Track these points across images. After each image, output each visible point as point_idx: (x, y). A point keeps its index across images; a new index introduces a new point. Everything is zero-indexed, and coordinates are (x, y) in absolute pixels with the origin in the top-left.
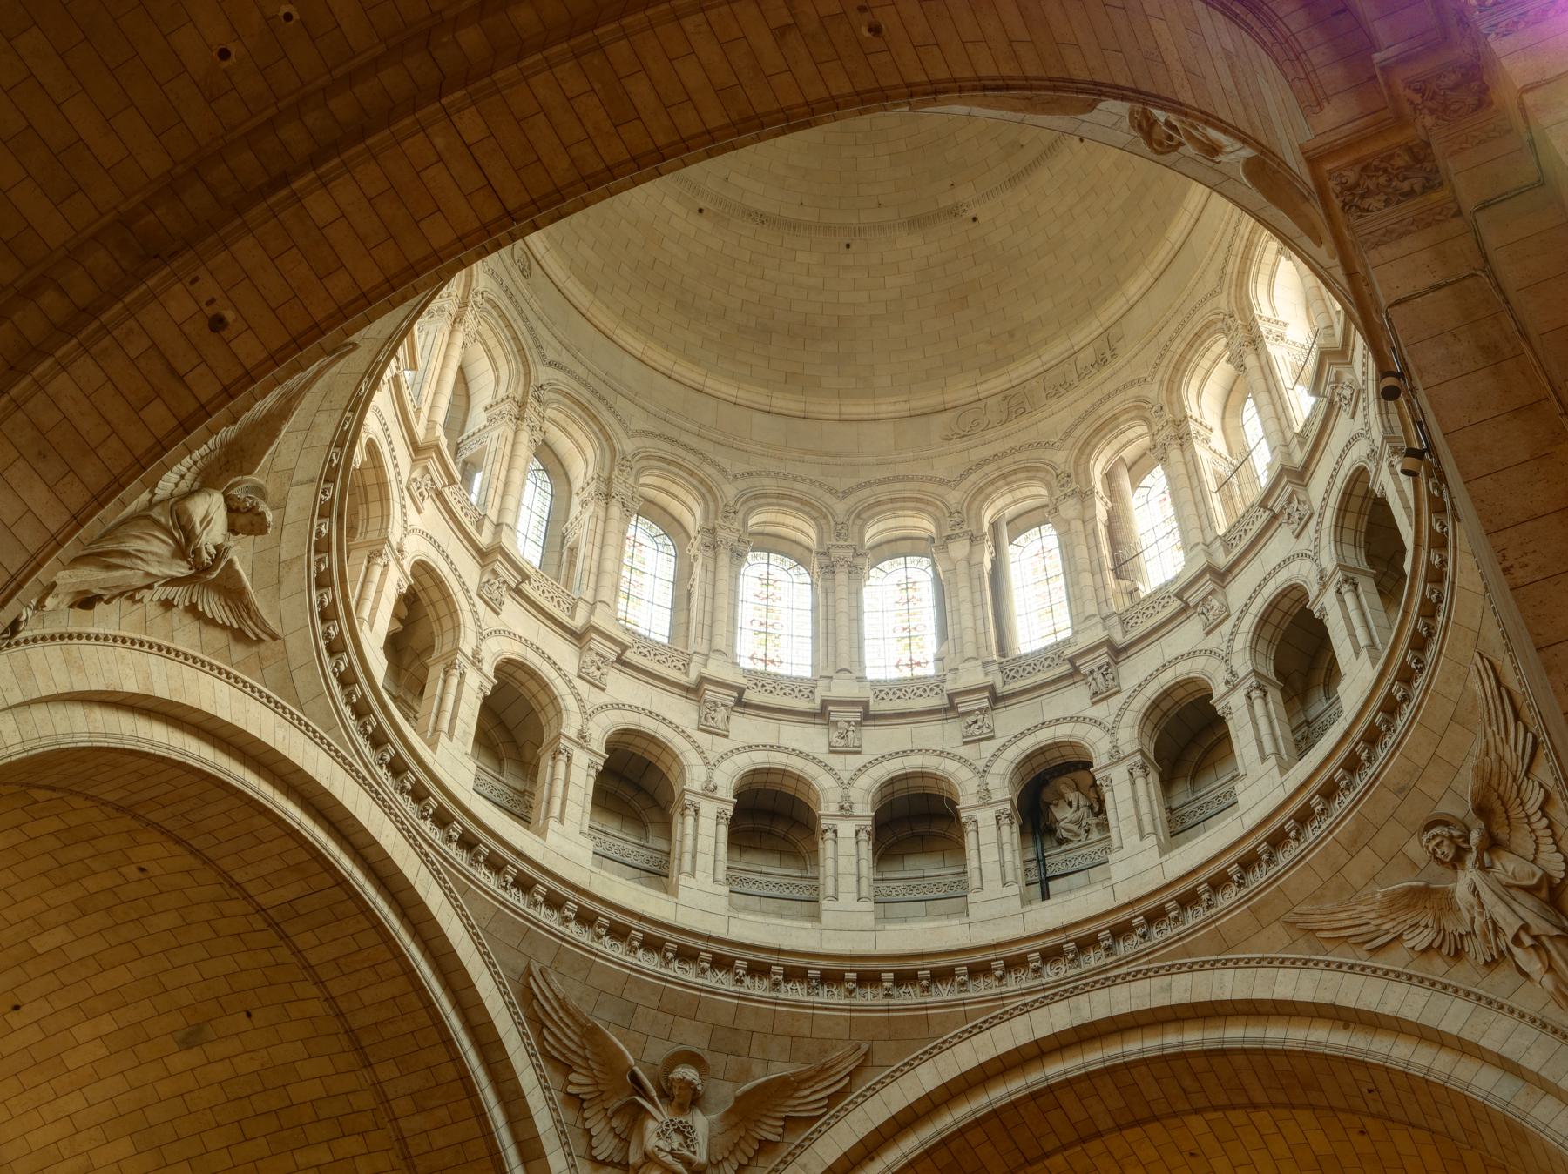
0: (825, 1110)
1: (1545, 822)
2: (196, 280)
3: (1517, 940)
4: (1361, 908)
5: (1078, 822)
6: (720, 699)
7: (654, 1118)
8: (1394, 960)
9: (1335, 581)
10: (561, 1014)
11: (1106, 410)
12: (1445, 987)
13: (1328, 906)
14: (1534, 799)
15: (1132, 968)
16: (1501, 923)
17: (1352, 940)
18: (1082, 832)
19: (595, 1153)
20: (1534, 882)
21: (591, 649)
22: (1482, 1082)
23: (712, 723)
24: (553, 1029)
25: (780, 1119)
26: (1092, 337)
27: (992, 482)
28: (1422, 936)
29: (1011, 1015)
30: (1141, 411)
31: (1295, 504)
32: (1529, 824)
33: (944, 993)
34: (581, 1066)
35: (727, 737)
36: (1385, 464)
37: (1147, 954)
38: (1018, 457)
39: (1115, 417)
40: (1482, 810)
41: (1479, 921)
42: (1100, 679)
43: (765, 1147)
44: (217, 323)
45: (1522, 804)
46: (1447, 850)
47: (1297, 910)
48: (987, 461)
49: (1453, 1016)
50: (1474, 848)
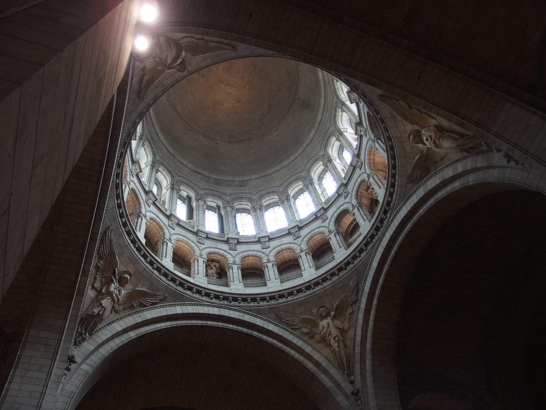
0: (150, 305)
1: (349, 316)
3: (334, 338)
4: (295, 318)
5: (212, 274)
6: (152, 198)
7: (114, 284)
8: (297, 333)
9: (306, 251)
10: (109, 244)
11: (241, 195)
12: (307, 342)
13: (288, 315)
14: (350, 311)
16: (332, 333)
17: (289, 324)
19: (94, 284)
20: (341, 327)
21: (135, 166)
23: (148, 202)
24: (105, 246)
26: (240, 180)
27: (210, 194)
28: (306, 330)
29: (203, 305)
30: (250, 200)
31: (297, 233)
32: (345, 316)
33: (189, 292)
34: (104, 260)
35: (150, 207)
36: (333, 234)
37: (240, 307)
38: (217, 193)
39: (242, 198)
40: (336, 309)
41: (325, 330)
42: (233, 246)
43: (132, 307)
45: (346, 311)
46: (324, 314)
47: (280, 312)
48: (210, 190)
49: (308, 349)
50: (332, 316)
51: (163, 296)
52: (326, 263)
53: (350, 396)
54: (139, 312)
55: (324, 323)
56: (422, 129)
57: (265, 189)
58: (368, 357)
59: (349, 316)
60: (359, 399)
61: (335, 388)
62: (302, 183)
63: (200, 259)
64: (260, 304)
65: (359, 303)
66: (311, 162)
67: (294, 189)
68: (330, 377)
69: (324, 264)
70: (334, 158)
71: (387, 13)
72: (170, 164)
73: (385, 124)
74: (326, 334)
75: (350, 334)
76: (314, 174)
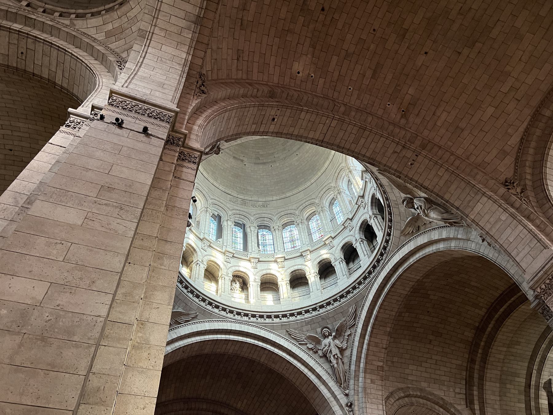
1: (347, 338)
2: (278, 110)
3: (334, 355)
8: (304, 347)
14: (348, 333)
15: (254, 324)
16: (332, 352)
18: (236, 290)
22: (312, 377)
25: (175, 320)
33: (216, 310)
38: (243, 213)
42: (255, 264)
44: (274, 119)
45: (345, 333)
47: (290, 329)
49: (312, 363)
51: (194, 315)
52: (331, 285)
53: (344, 407)
54: (175, 329)
55: (326, 341)
56: (415, 198)
57: (283, 211)
58: (362, 375)
59: (347, 338)
60: (351, 411)
61: (332, 399)
62: (315, 208)
63: (226, 277)
64: (273, 321)
65: (356, 328)
66: (323, 190)
67: (308, 212)
68: (329, 389)
69: (330, 285)
70: (343, 190)
71: (389, 105)
72: (204, 188)
73: (383, 188)
74: (327, 351)
75: (347, 353)
76: (326, 201)
